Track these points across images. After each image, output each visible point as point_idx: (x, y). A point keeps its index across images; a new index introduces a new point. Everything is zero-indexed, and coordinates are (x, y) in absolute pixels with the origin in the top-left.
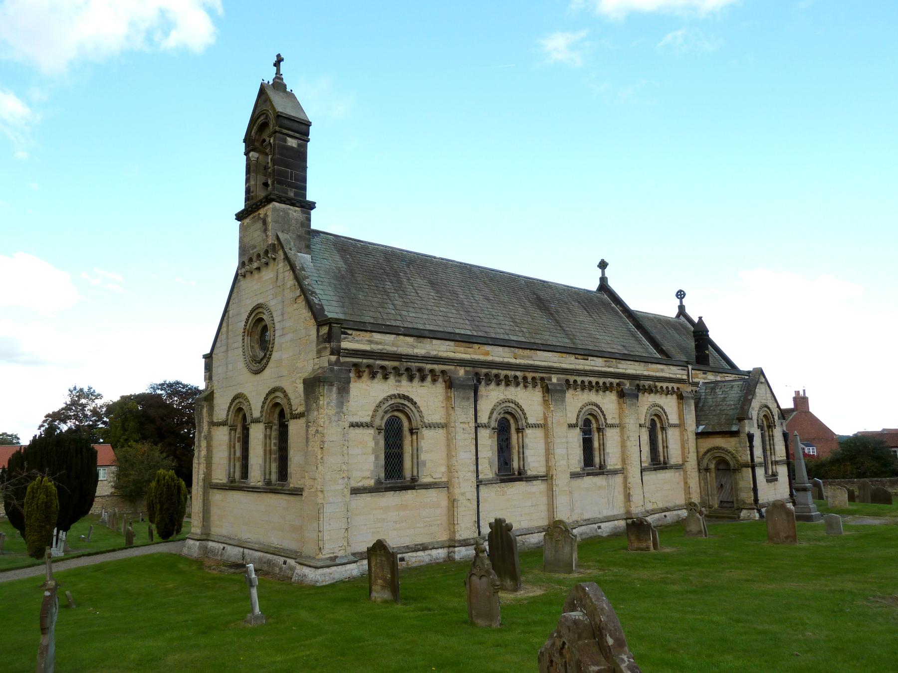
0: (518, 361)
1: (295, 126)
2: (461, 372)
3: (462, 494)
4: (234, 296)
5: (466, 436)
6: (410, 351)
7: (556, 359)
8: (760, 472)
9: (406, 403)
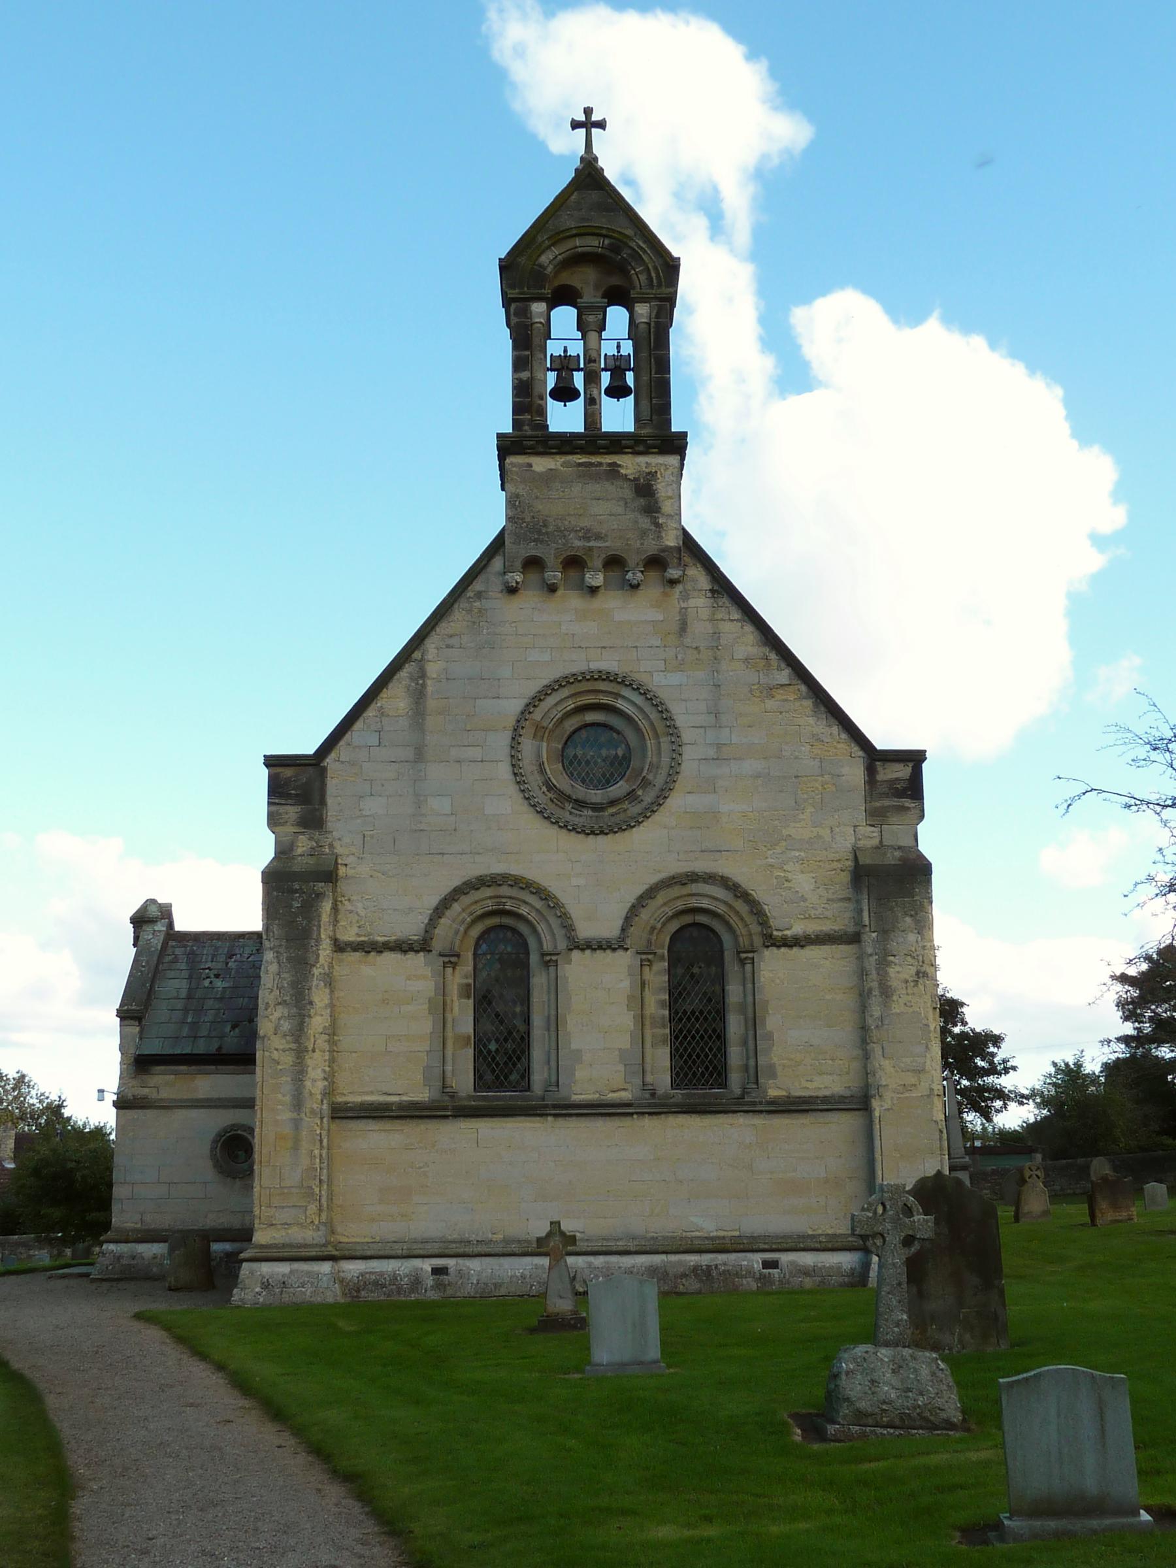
4: (443, 628)
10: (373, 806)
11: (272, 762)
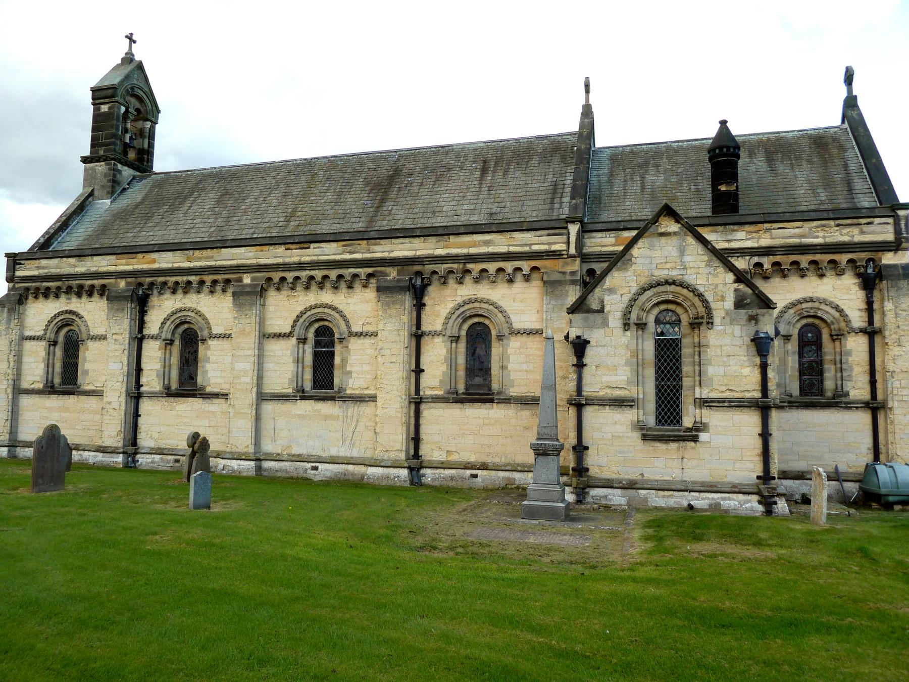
0: (192, 265)
2: (122, 284)
3: (110, 403)
5: (117, 347)
6: (71, 271)
7: (251, 255)
9: (74, 317)
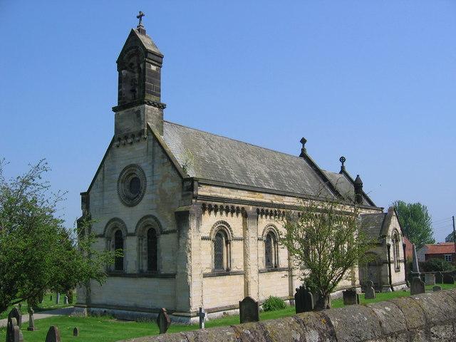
1: (156, 58)
2: (251, 208)
3: (252, 278)
4: (107, 158)
6: (228, 196)
8: (392, 266)
10: (96, 203)
11: (81, 194)
